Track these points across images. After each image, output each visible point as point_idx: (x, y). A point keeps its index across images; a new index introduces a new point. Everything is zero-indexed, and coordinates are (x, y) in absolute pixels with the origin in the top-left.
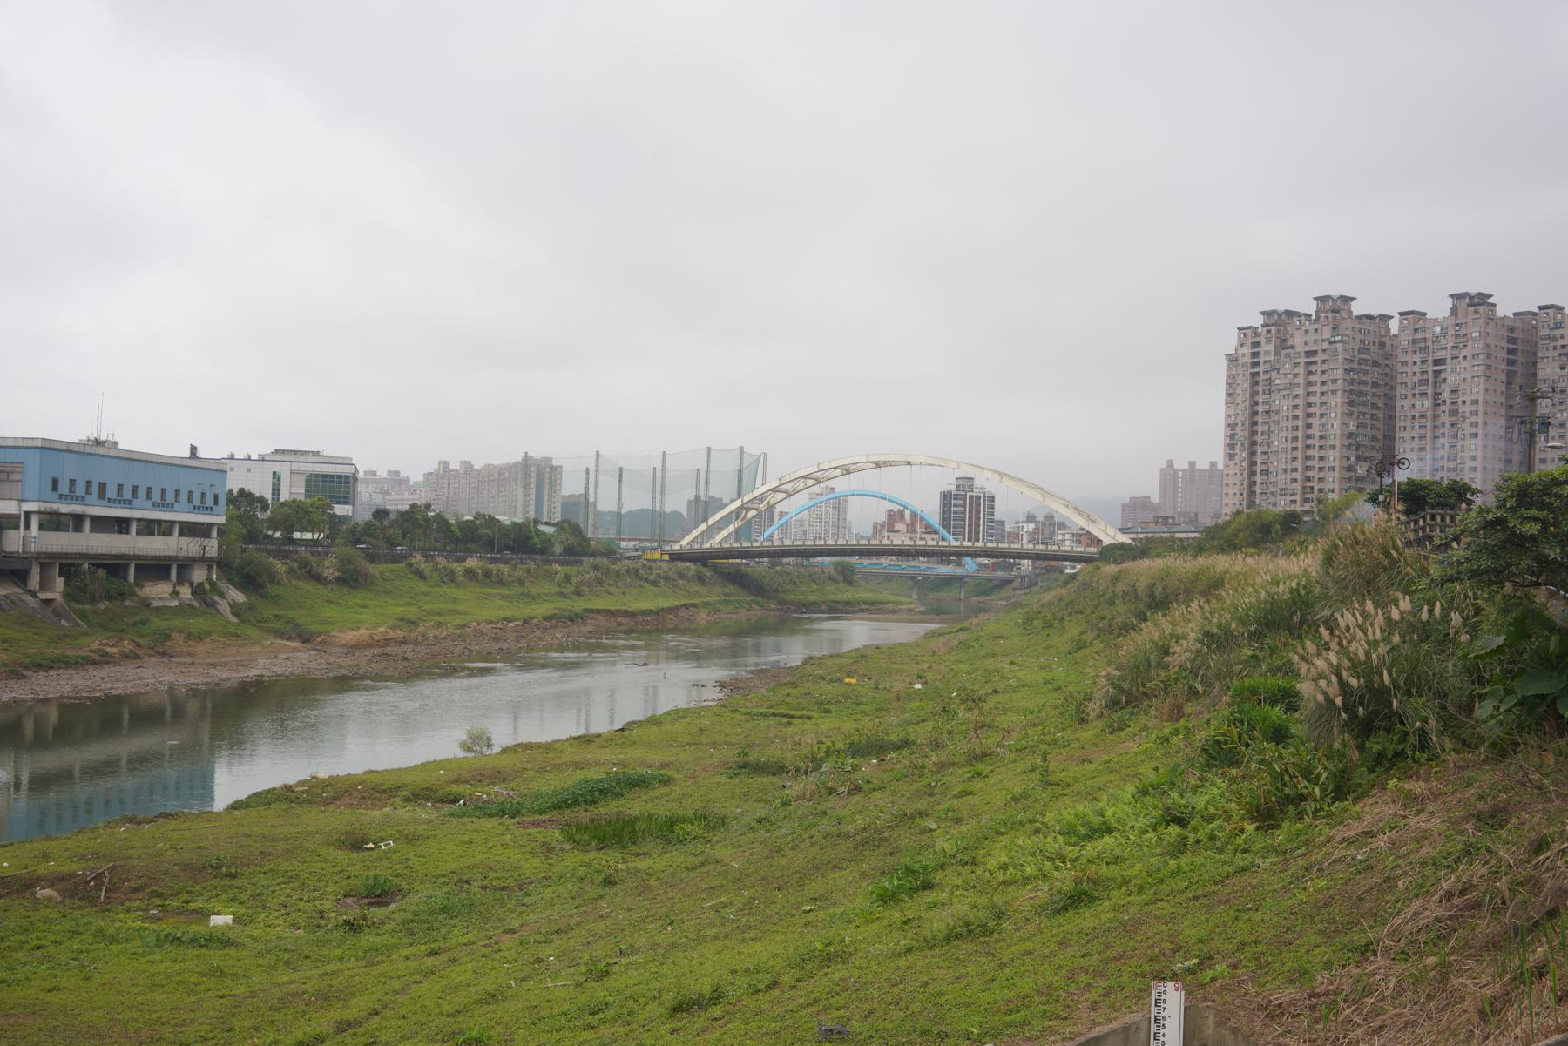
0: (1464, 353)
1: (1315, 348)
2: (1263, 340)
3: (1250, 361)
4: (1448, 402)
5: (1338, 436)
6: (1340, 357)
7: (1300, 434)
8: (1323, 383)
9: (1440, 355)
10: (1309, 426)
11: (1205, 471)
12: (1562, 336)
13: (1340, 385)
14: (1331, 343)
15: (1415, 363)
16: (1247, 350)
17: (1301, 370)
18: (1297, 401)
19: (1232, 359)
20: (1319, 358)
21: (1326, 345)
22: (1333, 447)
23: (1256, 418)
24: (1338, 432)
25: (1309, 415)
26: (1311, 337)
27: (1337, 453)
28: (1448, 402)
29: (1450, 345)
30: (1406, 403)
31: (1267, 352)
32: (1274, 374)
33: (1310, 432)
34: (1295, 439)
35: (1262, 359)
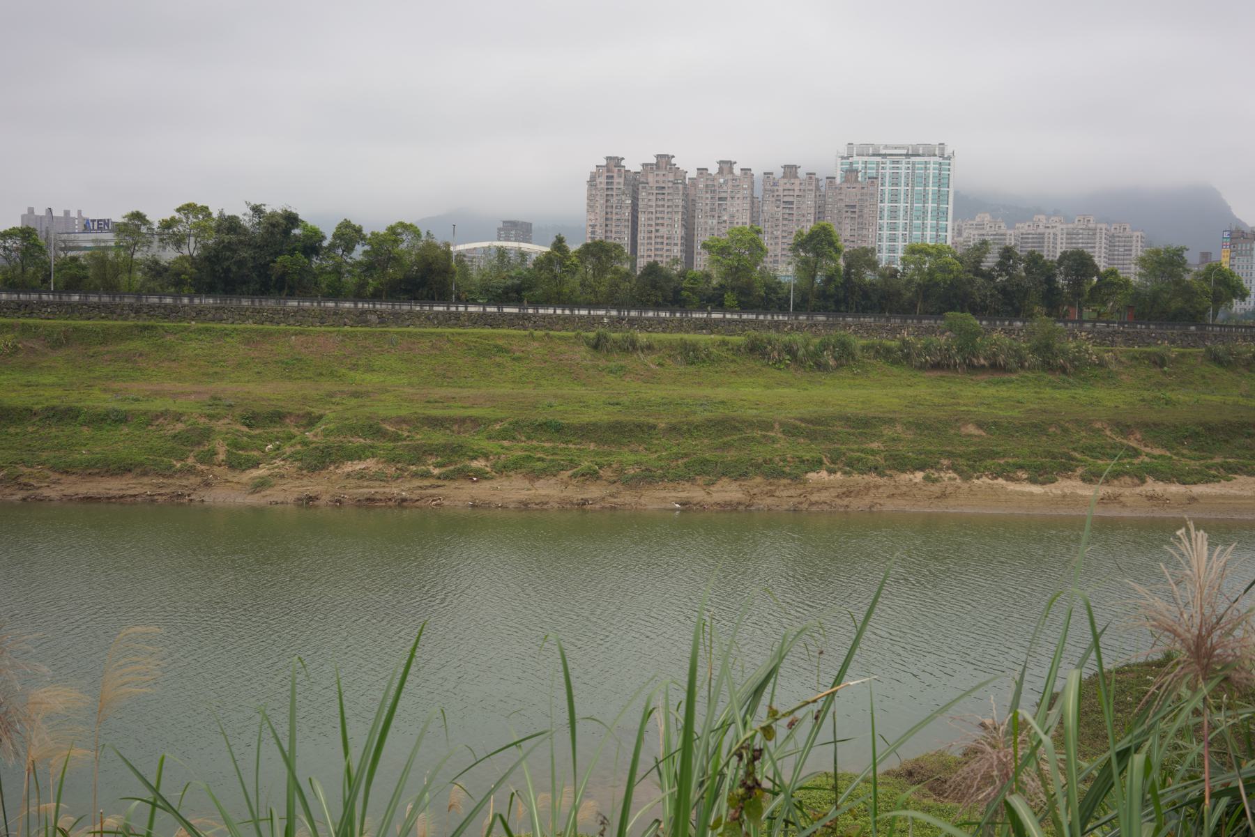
0: (738, 196)
1: (663, 185)
2: (615, 175)
3: (606, 187)
4: (728, 222)
5: (680, 238)
6: (681, 192)
7: (653, 236)
8: (668, 207)
9: (723, 195)
10: (657, 231)
11: (41, 217)
12: (777, 190)
13: (680, 209)
14: (674, 184)
15: (707, 198)
16: (603, 180)
17: (653, 198)
18: (650, 215)
19: (592, 182)
20: (666, 191)
21: (670, 185)
22: (676, 244)
23: (608, 222)
24: (680, 236)
25: (657, 225)
26: (661, 179)
27: (679, 248)
28: (728, 222)
29: (729, 191)
30: (702, 221)
31: (619, 183)
32: (623, 197)
33: (658, 234)
34: (650, 238)
35: (615, 187)
